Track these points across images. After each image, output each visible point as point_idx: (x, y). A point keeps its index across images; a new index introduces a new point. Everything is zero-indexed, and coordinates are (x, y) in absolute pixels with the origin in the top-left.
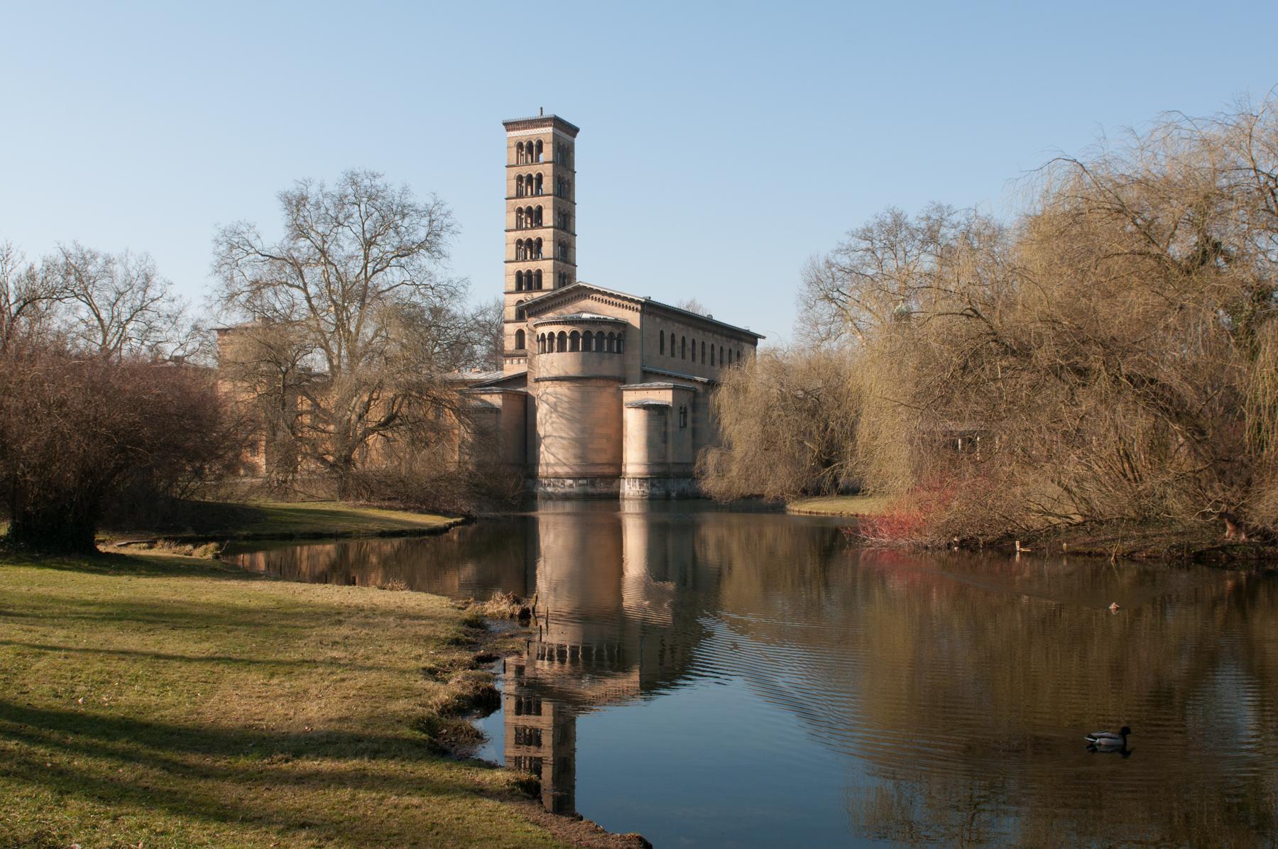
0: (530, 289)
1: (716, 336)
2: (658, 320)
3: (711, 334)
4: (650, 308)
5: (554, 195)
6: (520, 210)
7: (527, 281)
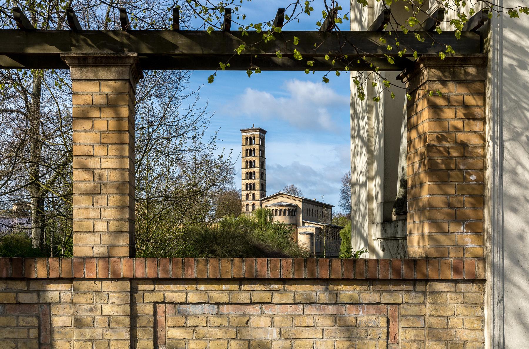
0: (250, 189)
6: (247, 162)
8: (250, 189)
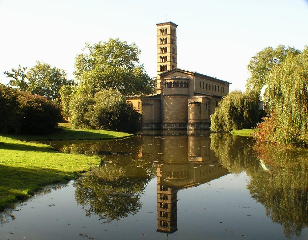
0: (164, 70)
1: (217, 83)
2: (199, 78)
3: (215, 82)
4: (196, 75)
5: (170, 44)
7: (163, 68)
8: (164, 70)
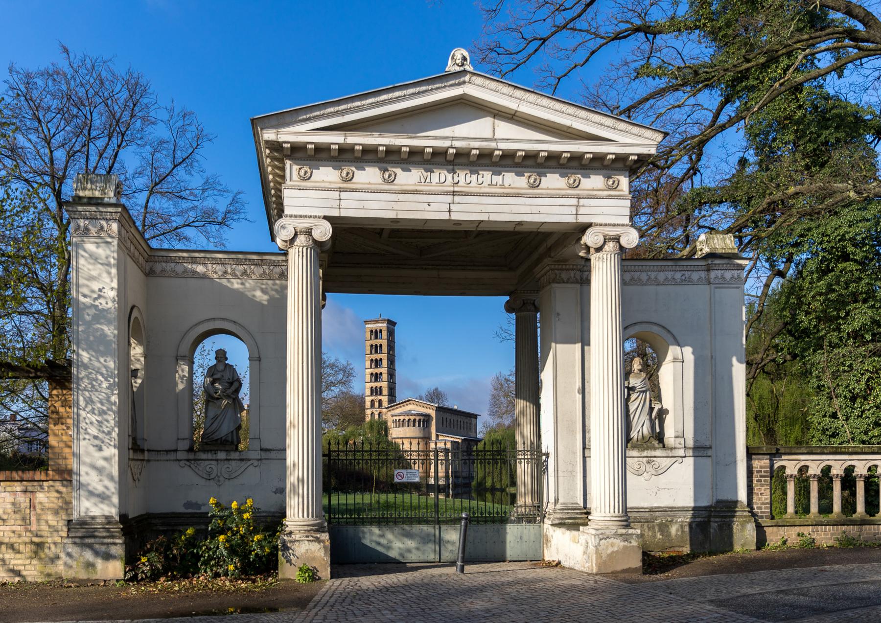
6: (372, 360)
